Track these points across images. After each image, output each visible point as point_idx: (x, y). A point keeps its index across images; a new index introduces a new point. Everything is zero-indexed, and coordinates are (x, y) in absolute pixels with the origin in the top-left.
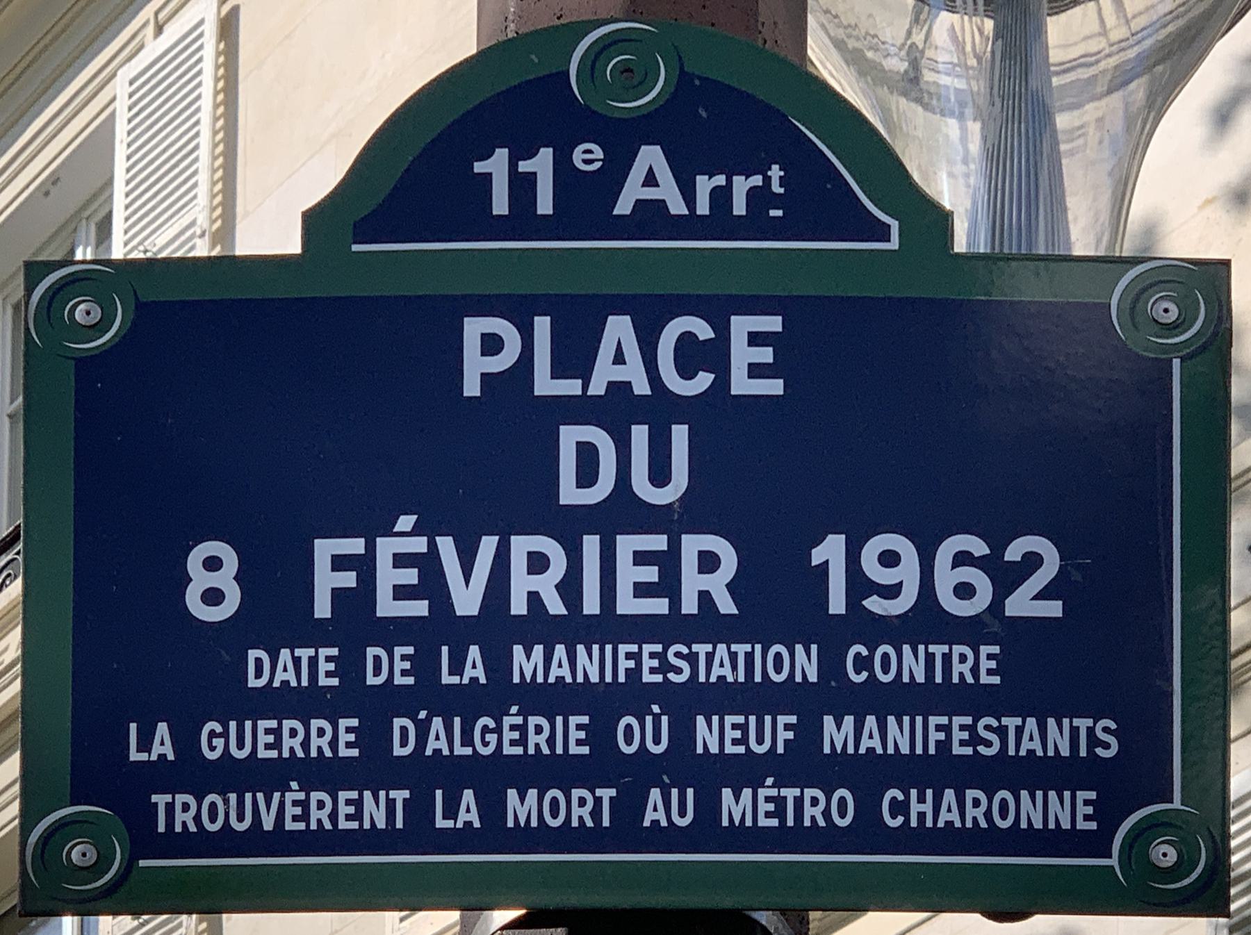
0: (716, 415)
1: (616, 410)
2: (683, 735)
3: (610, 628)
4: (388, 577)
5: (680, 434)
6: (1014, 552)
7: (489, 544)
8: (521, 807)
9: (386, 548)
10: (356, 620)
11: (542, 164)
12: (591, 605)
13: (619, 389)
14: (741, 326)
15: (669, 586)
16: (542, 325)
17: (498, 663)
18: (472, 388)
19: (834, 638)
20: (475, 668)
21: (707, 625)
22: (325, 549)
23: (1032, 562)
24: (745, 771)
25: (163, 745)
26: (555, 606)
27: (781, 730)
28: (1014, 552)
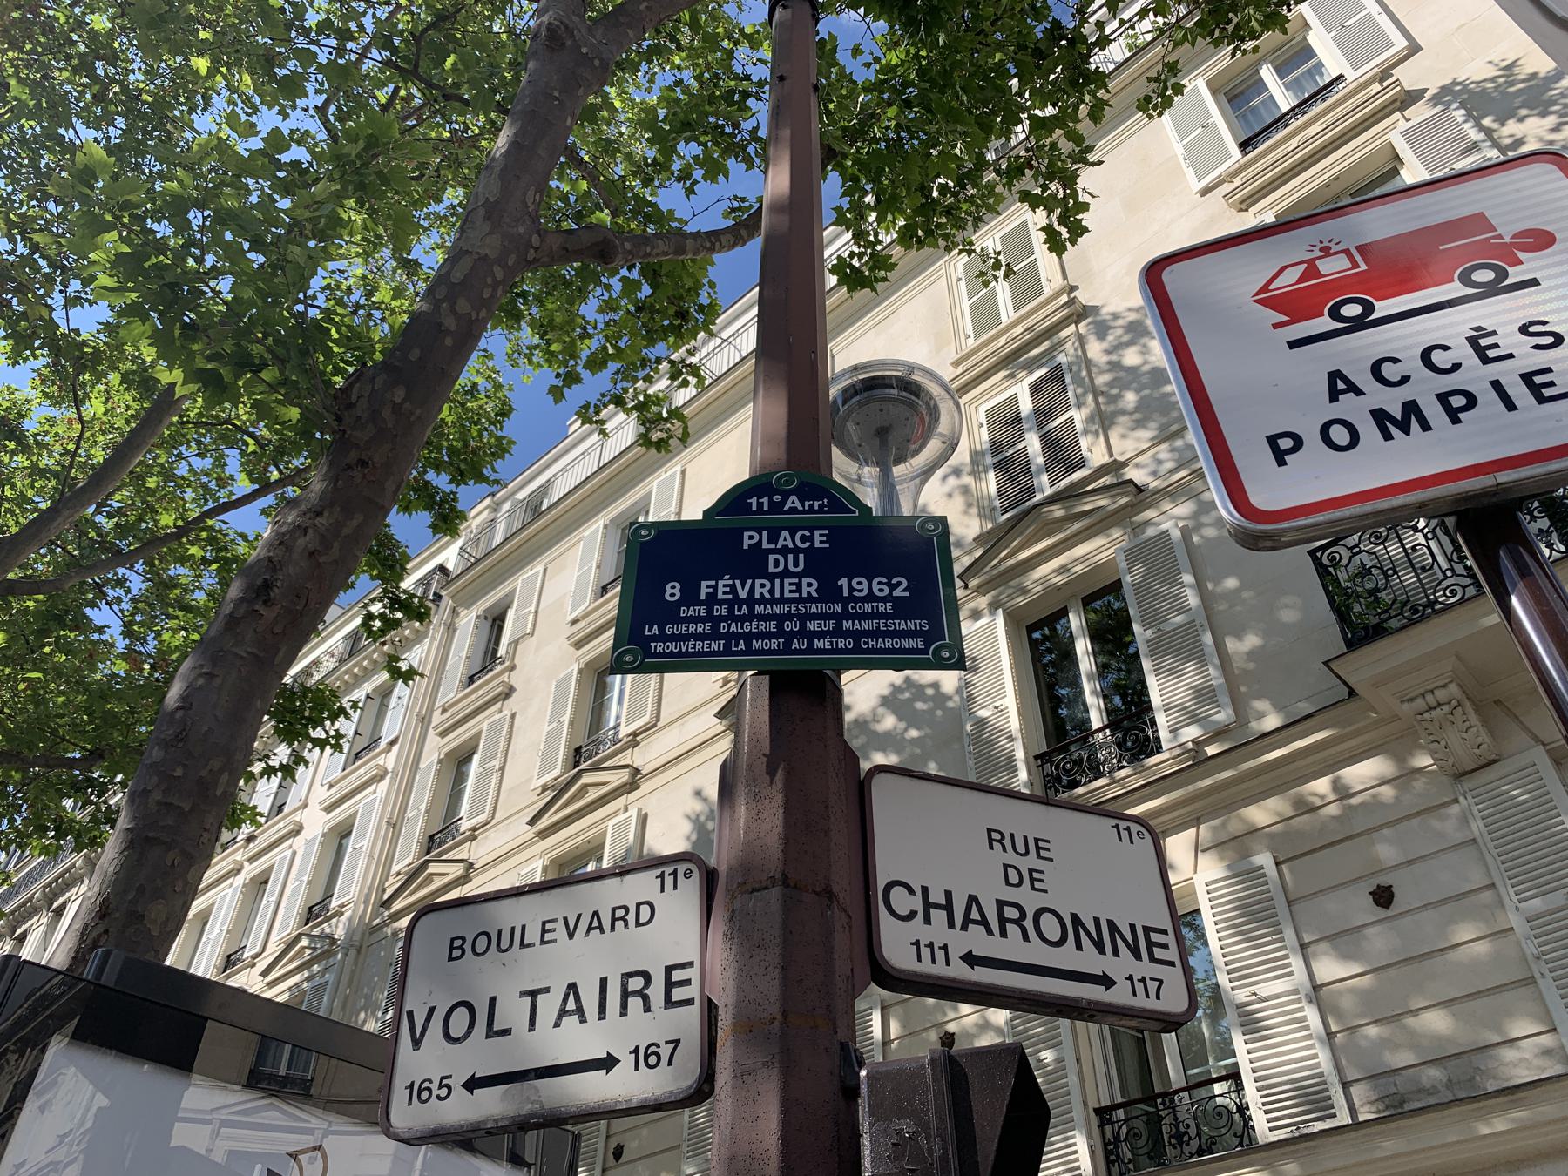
0: (811, 553)
1: (784, 551)
2: (803, 625)
3: (783, 600)
4: (721, 589)
5: (801, 556)
6: (894, 581)
7: (749, 582)
8: (756, 645)
9: (721, 583)
10: (712, 599)
11: (765, 500)
12: (777, 595)
13: (785, 547)
14: (817, 533)
15: (799, 590)
16: (765, 534)
17: (751, 609)
18: (746, 547)
19: (844, 602)
20: (745, 610)
21: (810, 599)
22: (704, 584)
23: (900, 583)
24: (821, 635)
25: (655, 630)
26: (767, 595)
27: (831, 624)
28: (894, 581)
